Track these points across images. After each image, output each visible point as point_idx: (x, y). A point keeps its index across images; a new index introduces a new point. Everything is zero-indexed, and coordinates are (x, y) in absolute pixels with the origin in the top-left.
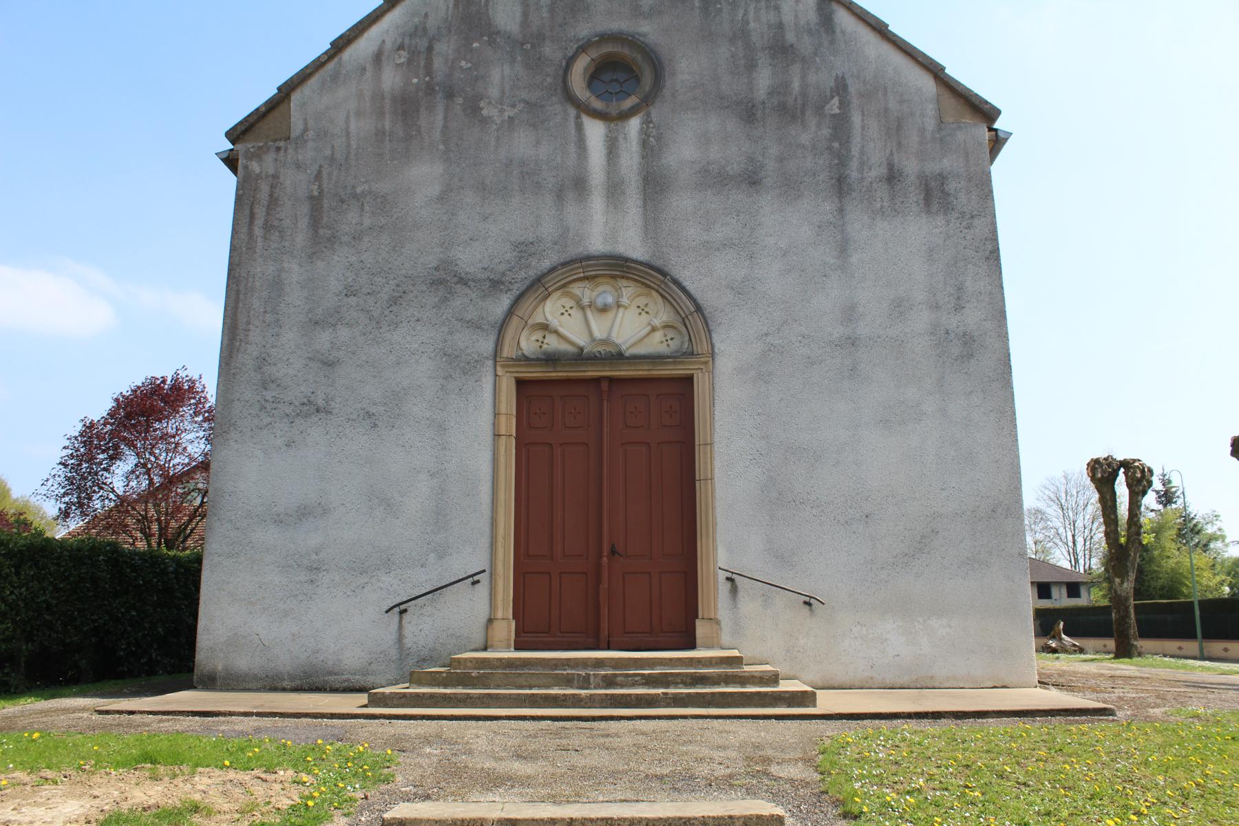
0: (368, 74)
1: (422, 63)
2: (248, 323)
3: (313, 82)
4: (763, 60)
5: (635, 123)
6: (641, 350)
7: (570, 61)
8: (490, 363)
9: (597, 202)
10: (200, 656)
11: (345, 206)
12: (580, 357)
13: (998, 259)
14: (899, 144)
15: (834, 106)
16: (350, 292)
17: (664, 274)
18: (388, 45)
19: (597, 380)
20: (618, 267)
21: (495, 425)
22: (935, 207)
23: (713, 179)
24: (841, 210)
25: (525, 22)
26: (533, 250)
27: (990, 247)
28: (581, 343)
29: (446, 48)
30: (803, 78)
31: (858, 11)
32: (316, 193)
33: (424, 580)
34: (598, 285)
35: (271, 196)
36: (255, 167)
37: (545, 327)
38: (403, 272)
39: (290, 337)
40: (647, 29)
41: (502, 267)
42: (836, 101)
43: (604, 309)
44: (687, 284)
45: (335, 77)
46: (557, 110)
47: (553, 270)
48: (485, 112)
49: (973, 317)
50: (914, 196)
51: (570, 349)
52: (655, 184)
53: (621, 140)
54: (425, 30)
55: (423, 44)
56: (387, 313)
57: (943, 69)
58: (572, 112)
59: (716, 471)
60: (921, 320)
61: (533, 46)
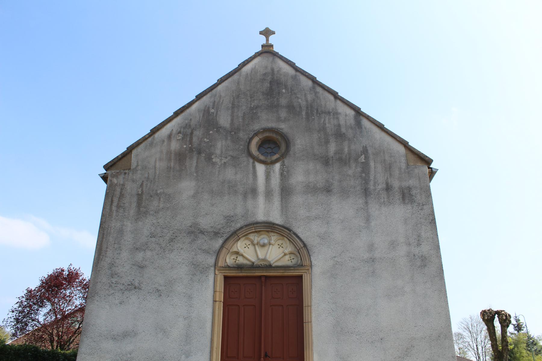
0: (165, 143)
1: (188, 139)
2: (107, 248)
3: (142, 146)
4: (332, 140)
5: (278, 166)
6: (280, 264)
7: (251, 139)
8: (213, 268)
9: (261, 199)
11: (152, 199)
12: (253, 267)
13: (435, 223)
14: (391, 175)
15: (362, 159)
16: (152, 236)
17: (290, 230)
18: (174, 132)
19: (260, 277)
20: (270, 227)
21: (214, 296)
22: (407, 201)
23: (311, 189)
24: (366, 203)
26: (233, 219)
27: (431, 218)
28: (253, 260)
29: (198, 133)
30: (349, 147)
31: (371, 120)
32: (140, 193)
34: (261, 235)
35: (121, 193)
36: (115, 181)
37: (237, 253)
38: (176, 228)
39: (125, 254)
40: (283, 127)
41: (219, 227)
42: (363, 156)
43: (263, 246)
44: (300, 235)
45: (151, 144)
46: (245, 160)
47: (241, 228)
48: (214, 160)
49: (425, 248)
50: (398, 196)
51: (248, 263)
52: (286, 192)
53: (272, 173)
54: (190, 126)
55: (189, 131)
56: (168, 245)
57: (408, 143)
58: (251, 161)
59: (313, 318)
60: (402, 250)
61: (235, 133)
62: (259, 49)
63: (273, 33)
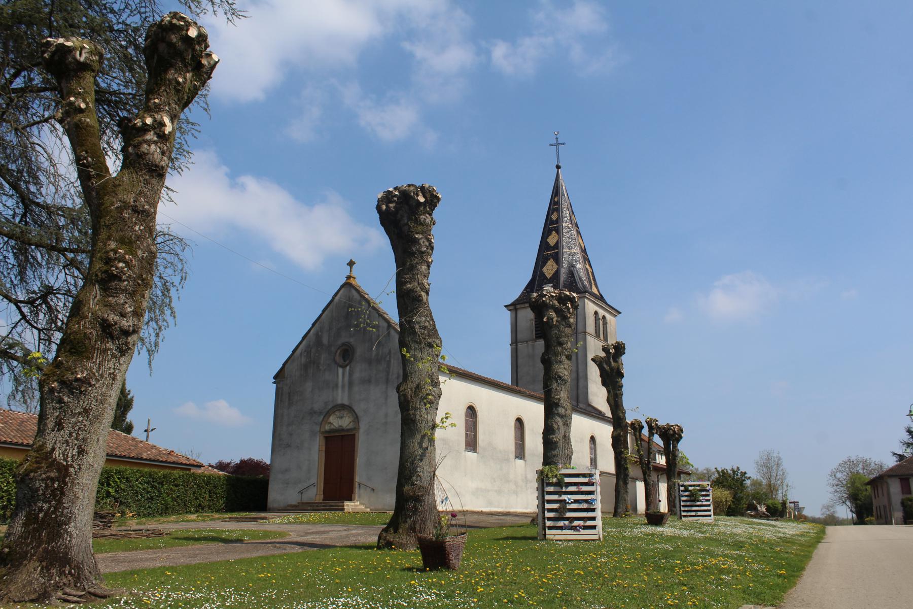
20: (343, 407)
29: (313, 350)
33: (306, 485)
40: (352, 340)
62: (344, 280)
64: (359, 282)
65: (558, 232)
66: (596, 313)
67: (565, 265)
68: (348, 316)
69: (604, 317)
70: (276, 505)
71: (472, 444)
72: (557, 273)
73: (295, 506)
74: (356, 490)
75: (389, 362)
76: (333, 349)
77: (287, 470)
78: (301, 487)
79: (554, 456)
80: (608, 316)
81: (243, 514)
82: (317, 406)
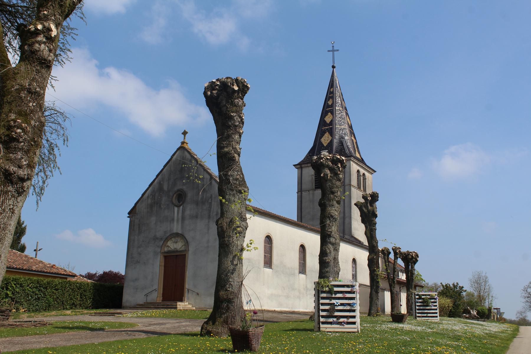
5: (181, 207)
6: (181, 249)
7: (173, 195)
10: (123, 303)
20: (177, 235)
25: (168, 188)
29: (157, 194)
33: (150, 290)
37: (168, 246)
40: (184, 188)
62: (179, 145)
63: (187, 133)
64: (191, 146)
65: (332, 113)
66: (358, 171)
67: (337, 137)
68: (182, 170)
69: (364, 174)
70: (128, 304)
71: (268, 262)
72: (331, 143)
73: (142, 305)
74: (186, 294)
75: (211, 203)
76: (171, 194)
77: (136, 280)
78: (146, 291)
79: (327, 272)
80: (367, 174)
81: (104, 310)
82: (159, 234)
